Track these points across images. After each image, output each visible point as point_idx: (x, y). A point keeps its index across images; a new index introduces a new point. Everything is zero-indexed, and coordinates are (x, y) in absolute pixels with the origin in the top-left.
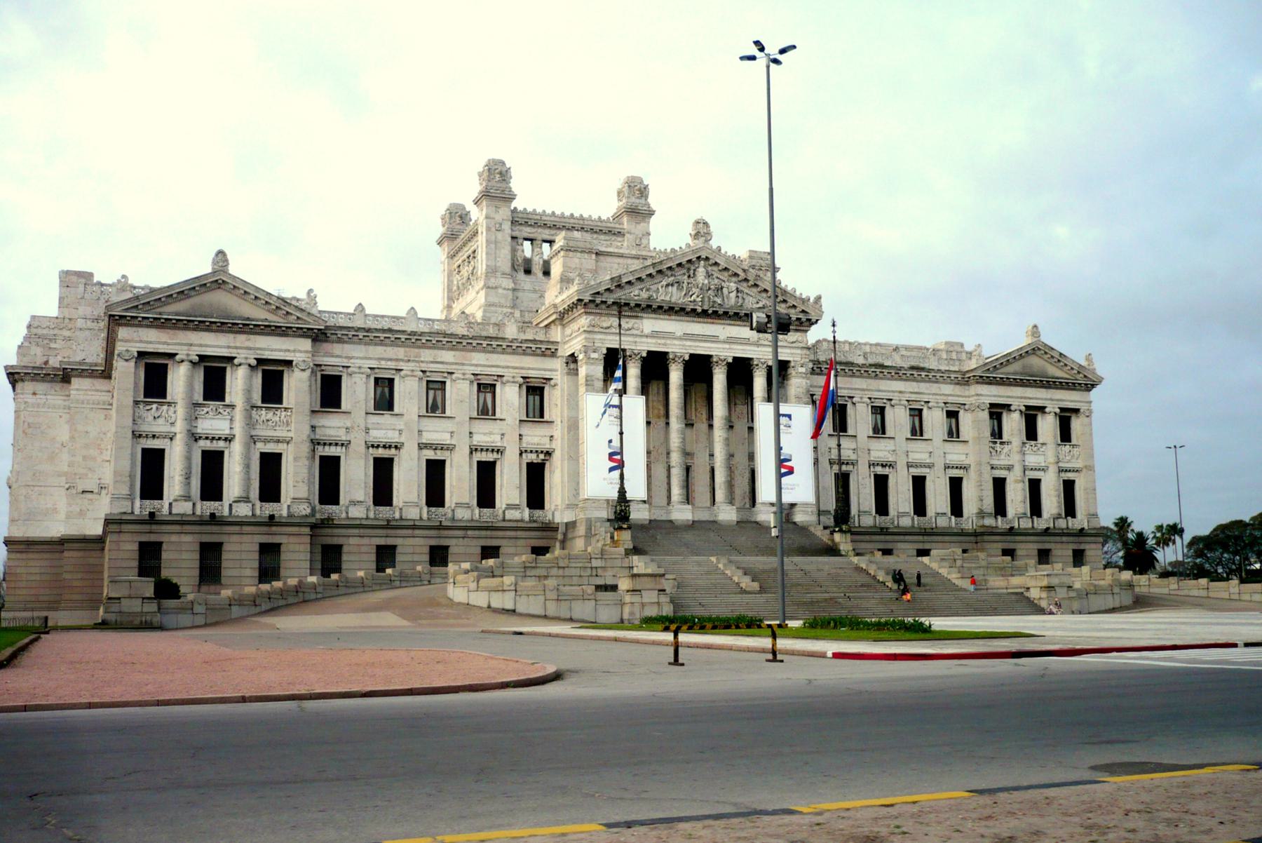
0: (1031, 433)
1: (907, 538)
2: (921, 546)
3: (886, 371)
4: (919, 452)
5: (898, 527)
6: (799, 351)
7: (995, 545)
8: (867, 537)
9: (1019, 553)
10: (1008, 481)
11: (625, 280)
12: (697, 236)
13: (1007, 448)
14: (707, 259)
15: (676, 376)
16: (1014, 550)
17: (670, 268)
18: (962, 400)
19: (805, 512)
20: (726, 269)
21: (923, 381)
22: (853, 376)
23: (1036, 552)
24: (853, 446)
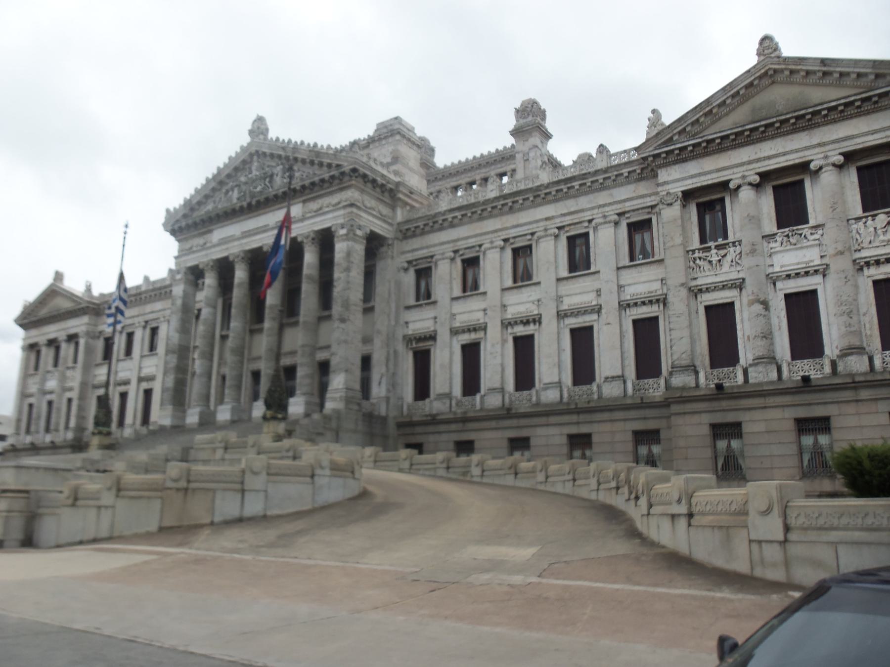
0: (791, 210)
1: (553, 419)
2: (574, 430)
3: (520, 199)
4: (580, 293)
5: (538, 404)
6: (342, 212)
7: (696, 419)
8: (493, 424)
9: (746, 428)
10: (737, 306)
11: (194, 201)
12: (251, 132)
13: (732, 252)
14: (257, 152)
15: (240, 274)
16: (738, 425)
17: (229, 176)
18: (649, 201)
19: (334, 399)
20: (272, 156)
21: (579, 194)
22: (481, 218)
23: (791, 425)
24: (483, 305)
